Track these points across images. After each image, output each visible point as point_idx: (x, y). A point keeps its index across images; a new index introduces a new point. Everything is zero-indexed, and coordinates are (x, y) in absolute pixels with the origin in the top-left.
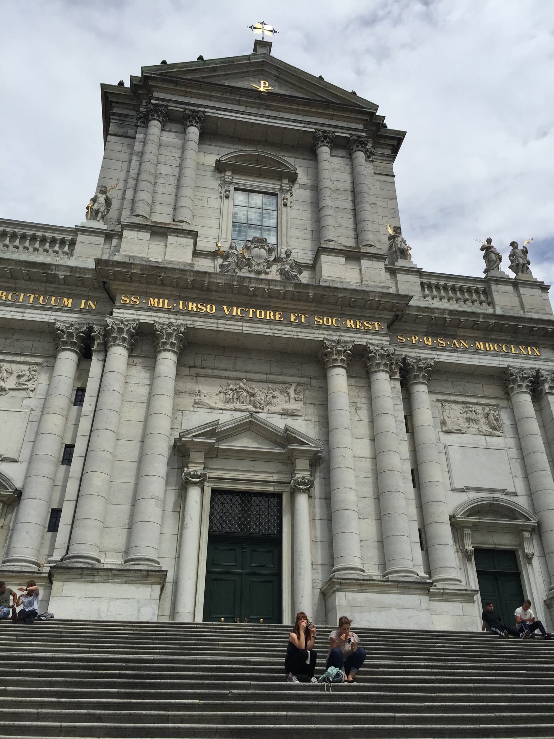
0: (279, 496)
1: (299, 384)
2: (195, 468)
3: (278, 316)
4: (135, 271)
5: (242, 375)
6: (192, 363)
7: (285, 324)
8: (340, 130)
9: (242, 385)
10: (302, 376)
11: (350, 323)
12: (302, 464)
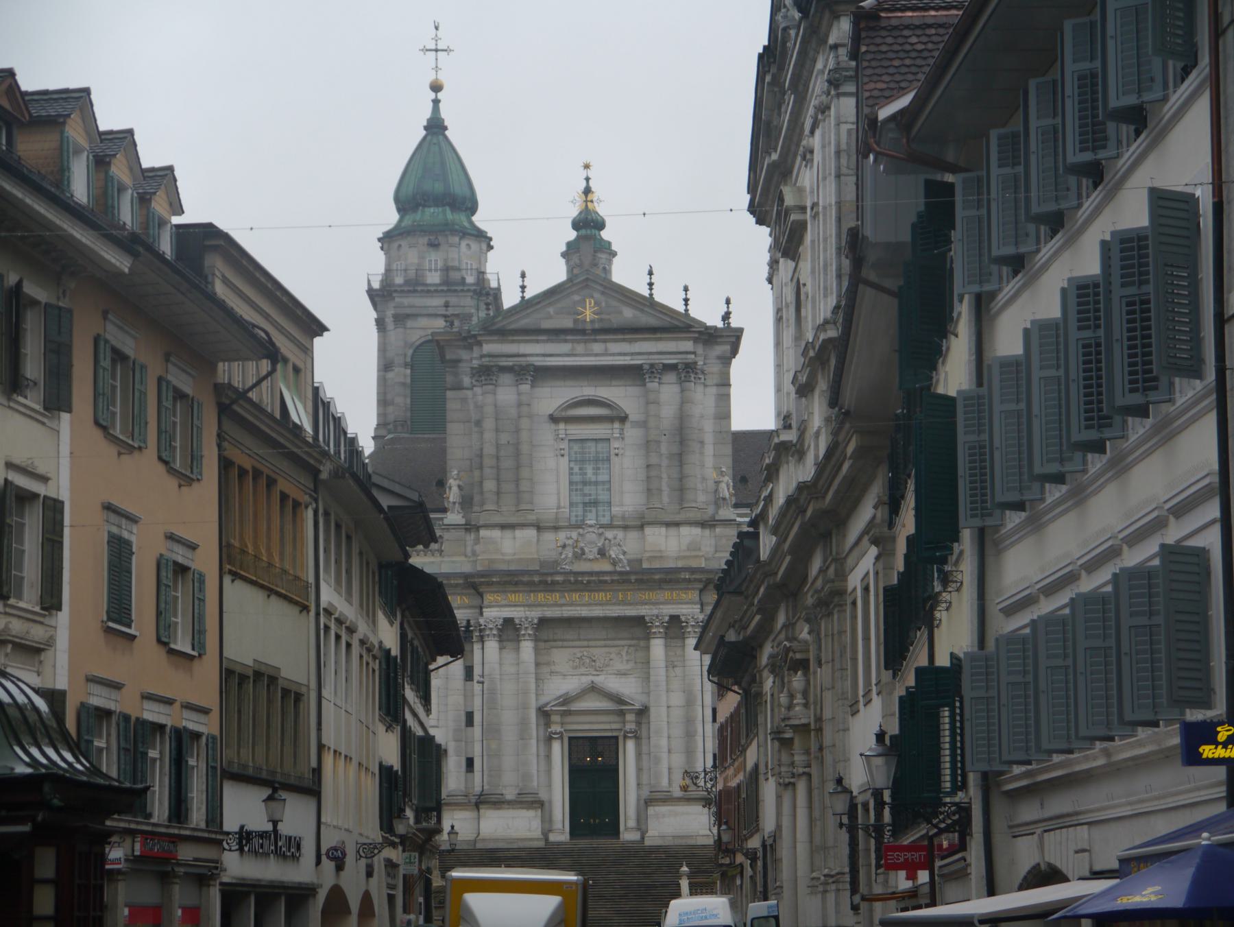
0: (616, 738)
1: (630, 646)
2: (556, 728)
3: (608, 597)
4: (495, 580)
5: (585, 643)
6: (546, 638)
7: (614, 604)
8: (668, 356)
9: (585, 653)
10: (632, 639)
11: (667, 594)
12: (630, 717)
